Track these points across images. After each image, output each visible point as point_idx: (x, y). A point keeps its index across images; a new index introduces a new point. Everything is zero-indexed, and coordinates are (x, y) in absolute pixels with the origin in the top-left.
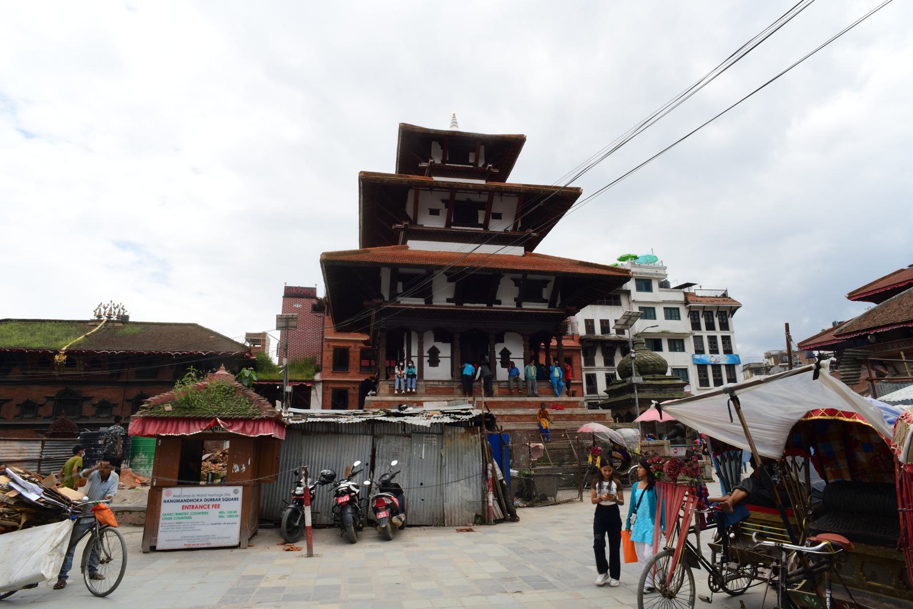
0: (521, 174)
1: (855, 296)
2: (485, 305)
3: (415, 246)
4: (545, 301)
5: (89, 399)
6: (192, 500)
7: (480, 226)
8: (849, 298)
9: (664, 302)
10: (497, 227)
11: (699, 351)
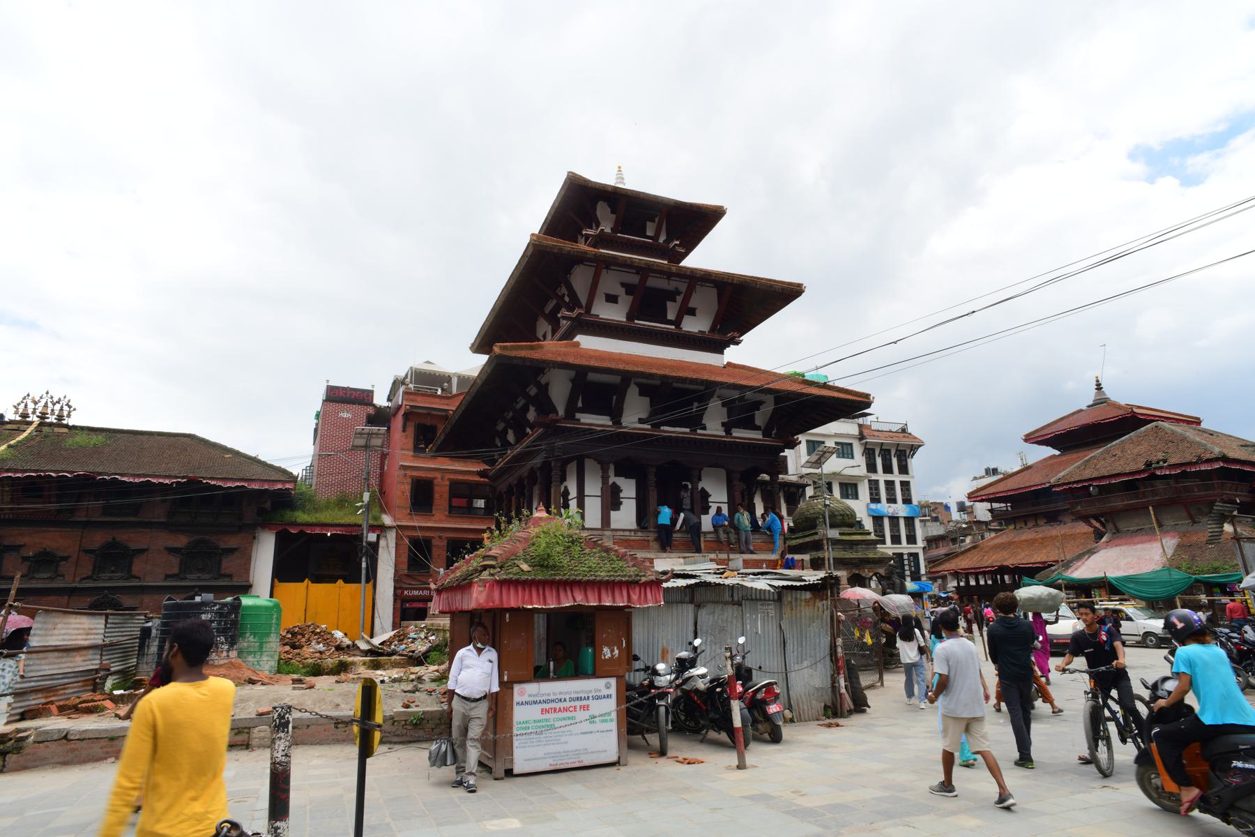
0: (706, 256)
1: (1034, 438)
2: (688, 430)
3: (589, 343)
4: (757, 428)
5: (16, 548)
6: (553, 701)
7: (670, 322)
8: (1026, 440)
9: (836, 435)
10: (692, 325)
11: (875, 499)
